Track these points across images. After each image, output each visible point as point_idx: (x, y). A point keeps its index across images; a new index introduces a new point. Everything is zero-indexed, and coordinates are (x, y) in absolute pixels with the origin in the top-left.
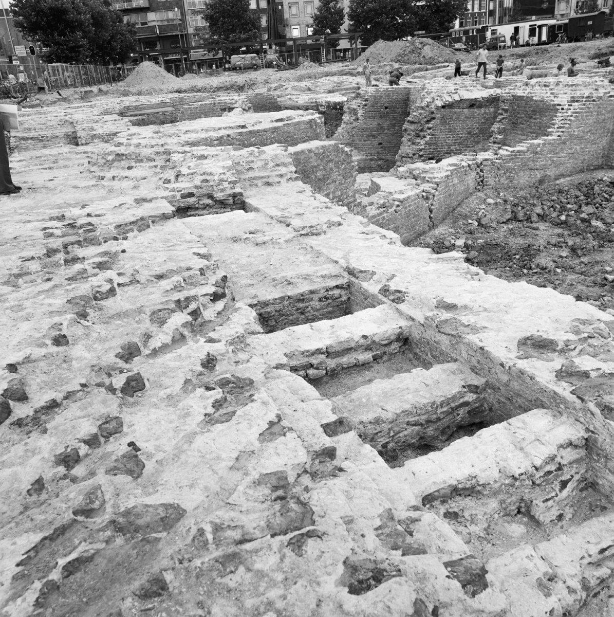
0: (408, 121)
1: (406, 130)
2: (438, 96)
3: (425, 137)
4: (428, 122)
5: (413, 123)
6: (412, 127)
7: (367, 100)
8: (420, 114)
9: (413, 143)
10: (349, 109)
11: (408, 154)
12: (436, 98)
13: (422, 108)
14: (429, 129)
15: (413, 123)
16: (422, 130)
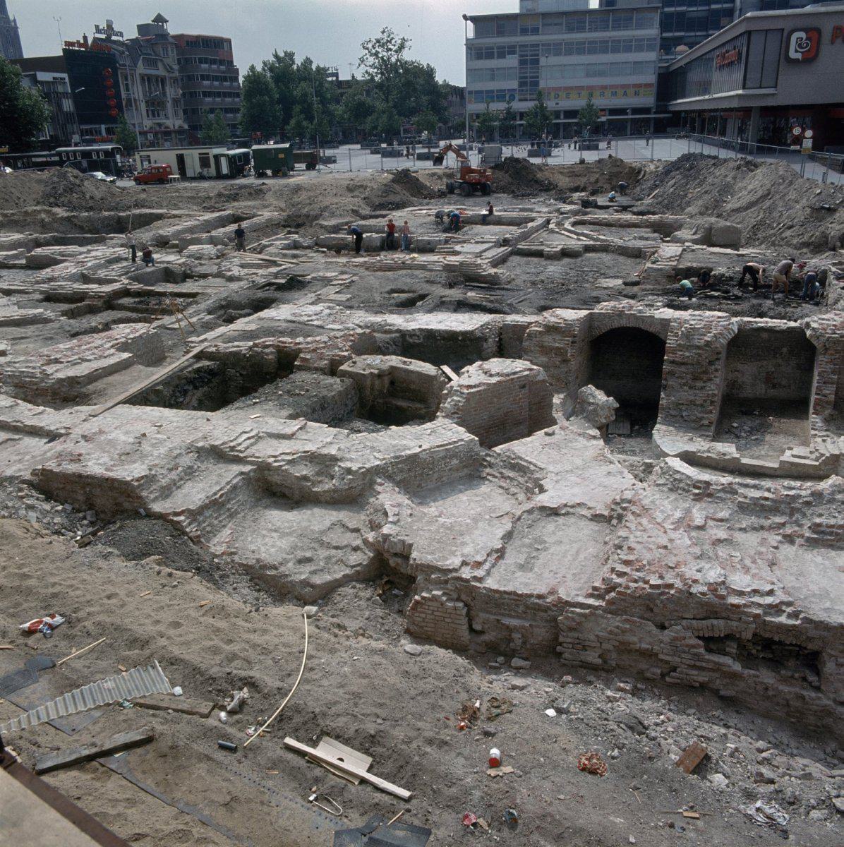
0: (673, 362)
1: (671, 373)
2: (720, 334)
3: (710, 380)
4: (711, 363)
5: (683, 364)
6: (683, 369)
7: (575, 336)
8: (700, 355)
9: (691, 388)
10: (542, 347)
11: (691, 401)
12: (718, 336)
13: (698, 347)
14: (716, 370)
15: (683, 364)
16: (705, 372)
